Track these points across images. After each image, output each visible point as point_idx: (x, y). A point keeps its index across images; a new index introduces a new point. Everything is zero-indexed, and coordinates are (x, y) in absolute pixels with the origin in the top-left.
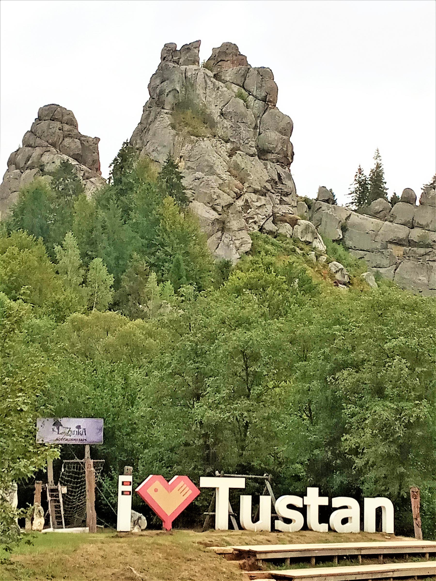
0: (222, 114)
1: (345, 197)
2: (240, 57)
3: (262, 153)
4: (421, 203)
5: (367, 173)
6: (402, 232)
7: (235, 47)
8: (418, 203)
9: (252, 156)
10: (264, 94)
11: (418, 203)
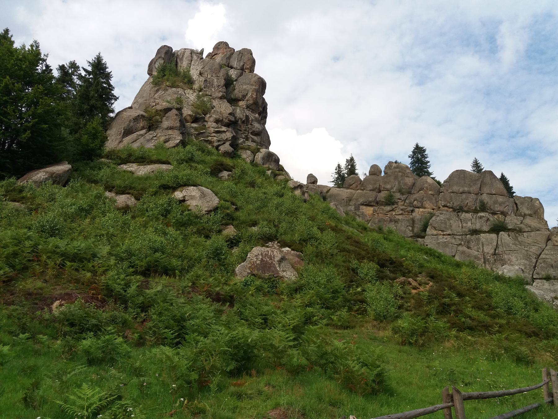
0: (201, 74)
1: (327, 179)
2: (229, 50)
3: (233, 101)
4: (385, 173)
5: (343, 165)
6: (371, 196)
7: (226, 44)
8: (383, 174)
9: (221, 98)
10: (242, 64)
11: (383, 174)
